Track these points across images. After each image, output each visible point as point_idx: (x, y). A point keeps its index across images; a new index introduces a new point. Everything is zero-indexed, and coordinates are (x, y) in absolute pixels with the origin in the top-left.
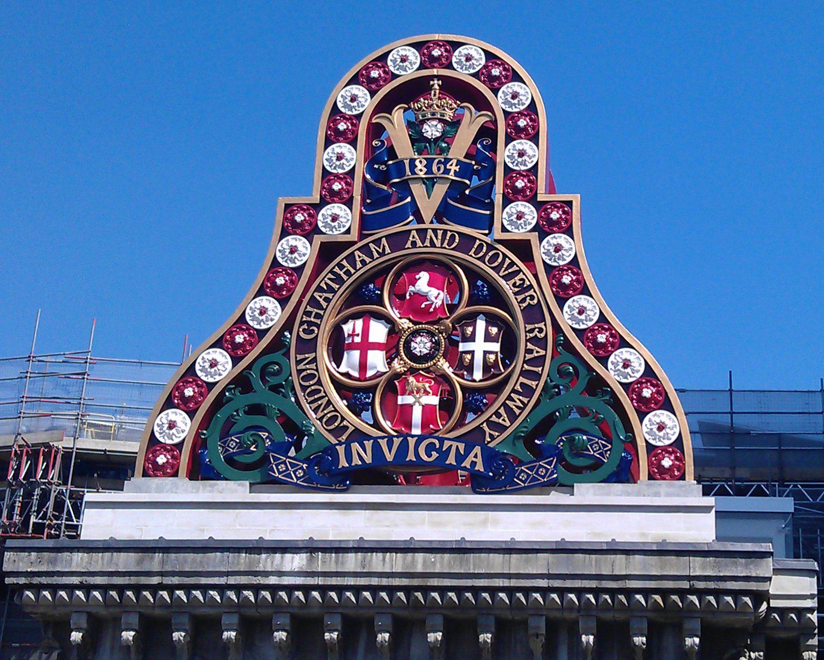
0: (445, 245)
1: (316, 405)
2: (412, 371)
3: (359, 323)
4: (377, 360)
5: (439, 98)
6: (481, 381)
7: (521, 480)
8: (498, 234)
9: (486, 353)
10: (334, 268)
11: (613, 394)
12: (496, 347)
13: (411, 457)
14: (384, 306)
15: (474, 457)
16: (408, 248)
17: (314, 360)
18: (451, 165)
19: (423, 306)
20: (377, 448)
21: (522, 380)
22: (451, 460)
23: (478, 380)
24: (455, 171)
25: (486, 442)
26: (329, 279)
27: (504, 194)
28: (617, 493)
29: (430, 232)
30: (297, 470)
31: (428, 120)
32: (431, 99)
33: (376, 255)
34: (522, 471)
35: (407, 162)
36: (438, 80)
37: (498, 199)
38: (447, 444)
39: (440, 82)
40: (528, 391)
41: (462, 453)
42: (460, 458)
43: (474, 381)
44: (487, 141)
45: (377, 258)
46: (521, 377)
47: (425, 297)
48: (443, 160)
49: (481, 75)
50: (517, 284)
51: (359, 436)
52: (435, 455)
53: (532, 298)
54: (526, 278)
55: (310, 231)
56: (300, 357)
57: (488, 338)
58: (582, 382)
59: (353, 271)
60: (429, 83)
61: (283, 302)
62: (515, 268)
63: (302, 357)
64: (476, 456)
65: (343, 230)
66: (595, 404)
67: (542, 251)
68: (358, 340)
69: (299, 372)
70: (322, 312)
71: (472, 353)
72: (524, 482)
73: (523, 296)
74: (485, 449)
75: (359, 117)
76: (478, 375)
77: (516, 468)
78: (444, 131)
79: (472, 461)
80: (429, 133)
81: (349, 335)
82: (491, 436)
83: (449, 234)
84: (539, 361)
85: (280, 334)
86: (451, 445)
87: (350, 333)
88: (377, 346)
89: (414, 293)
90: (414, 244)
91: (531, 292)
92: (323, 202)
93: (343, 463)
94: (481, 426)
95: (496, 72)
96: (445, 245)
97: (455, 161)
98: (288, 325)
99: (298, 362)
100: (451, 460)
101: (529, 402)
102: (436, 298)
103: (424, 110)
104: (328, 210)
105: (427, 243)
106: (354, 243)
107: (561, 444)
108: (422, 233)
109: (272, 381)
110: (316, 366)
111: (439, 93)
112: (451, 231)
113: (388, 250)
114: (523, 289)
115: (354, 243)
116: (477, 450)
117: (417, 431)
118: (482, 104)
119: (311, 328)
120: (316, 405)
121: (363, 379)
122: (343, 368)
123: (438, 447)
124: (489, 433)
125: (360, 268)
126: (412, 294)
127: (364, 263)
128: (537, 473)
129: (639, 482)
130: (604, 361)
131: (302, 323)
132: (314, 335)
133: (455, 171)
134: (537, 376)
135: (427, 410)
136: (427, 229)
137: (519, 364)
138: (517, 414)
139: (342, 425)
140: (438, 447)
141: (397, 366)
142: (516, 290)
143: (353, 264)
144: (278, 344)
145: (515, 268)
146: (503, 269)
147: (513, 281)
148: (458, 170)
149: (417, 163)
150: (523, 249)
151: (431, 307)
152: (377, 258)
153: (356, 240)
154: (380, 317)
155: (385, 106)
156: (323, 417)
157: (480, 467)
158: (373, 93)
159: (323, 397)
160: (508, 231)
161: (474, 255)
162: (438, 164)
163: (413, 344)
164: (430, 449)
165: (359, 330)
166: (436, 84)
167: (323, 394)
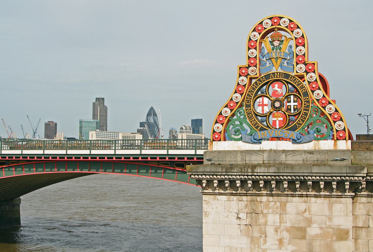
3: (261, 98)
8: (295, 73)
9: (294, 106)
11: (326, 116)
31: (275, 40)
37: (295, 64)
57: (294, 102)
62: (300, 82)
63: (247, 108)
65: (255, 74)
67: (307, 78)
68: (261, 103)
69: (247, 112)
71: (290, 106)
75: (256, 41)
76: (292, 111)
80: (275, 45)
85: (242, 102)
92: (249, 66)
98: (243, 100)
99: (246, 110)
104: (251, 69)
144: (241, 106)
147: (300, 86)
150: (302, 77)
158: (260, 34)
160: (298, 73)
165: (261, 101)
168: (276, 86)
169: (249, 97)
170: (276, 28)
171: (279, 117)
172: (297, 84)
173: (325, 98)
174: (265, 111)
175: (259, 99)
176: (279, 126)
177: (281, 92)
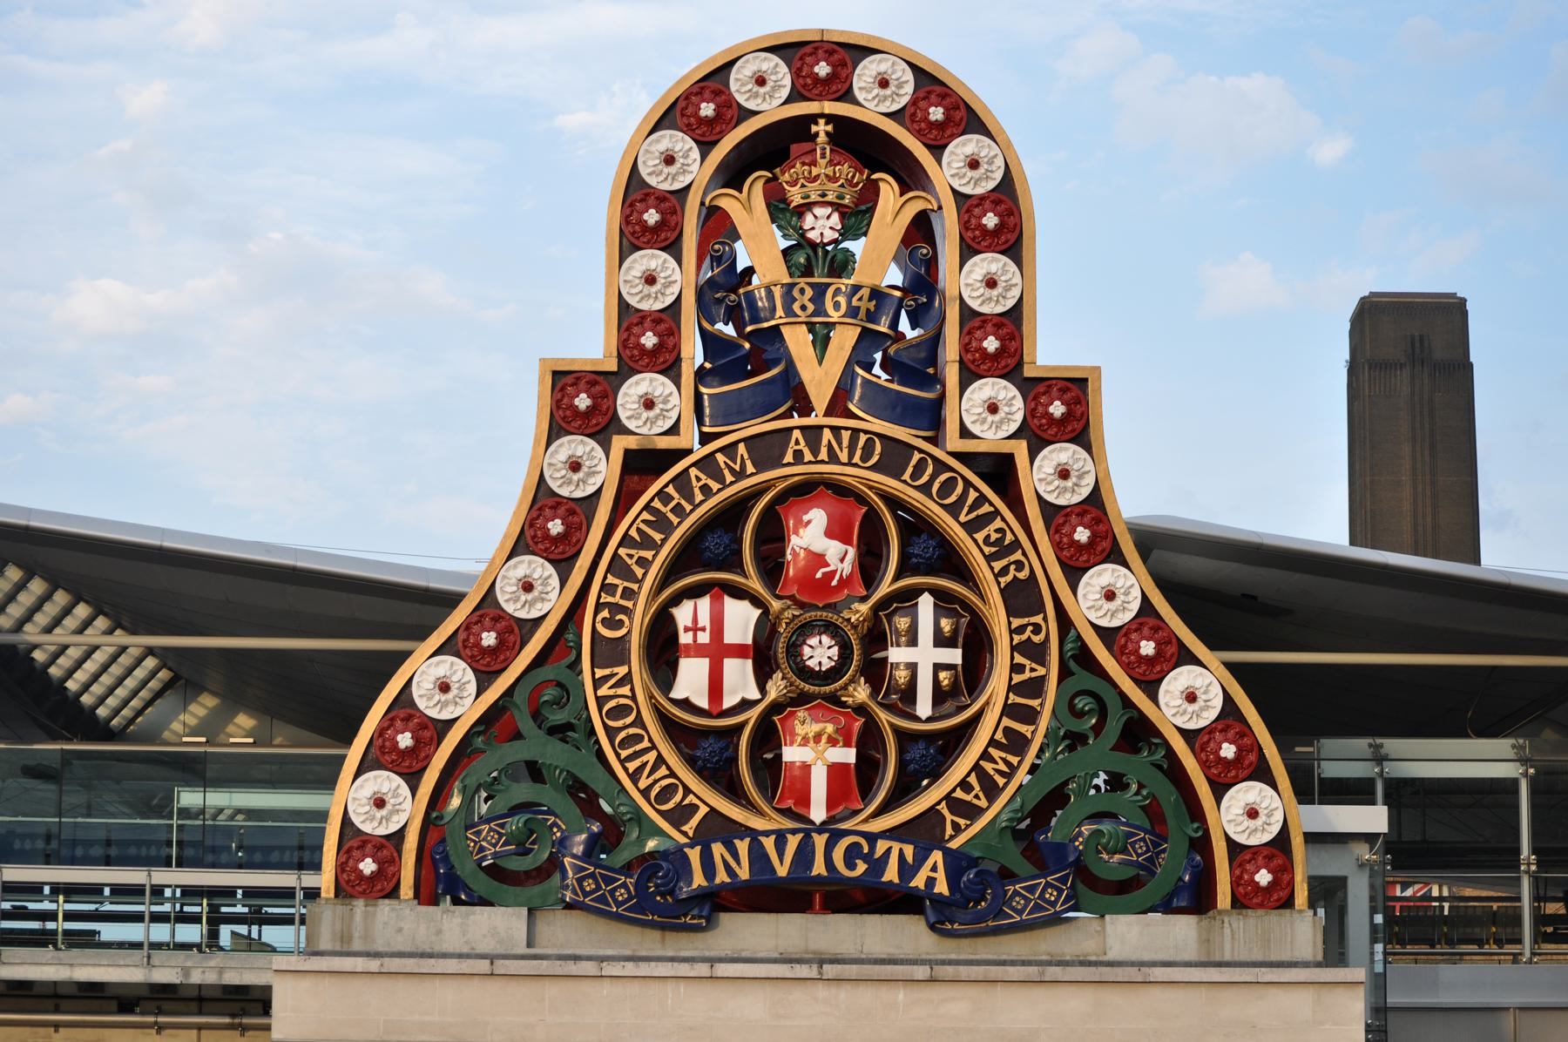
0: (856, 459)
2: (801, 699)
4: (740, 680)
5: (831, 163)
6: (929, 720)
7: (1013, 909)
8: (954, 442)
9: (938, 667)
10: (652, 500)
12: (955, 656)
13: (819, 868)
15: (931, 870)
16: (789, 464)
17: (627, 679)
18: (860, 299)
19: (819, 575)
20: (757, 854)
21: (1006, 722)
22: (891, 874)
23: (924, 717)
24: (868, 310)
25: (947, 837)
26: (643, 521)
27: (961, 362)
28: (1180, 932)
29: (827, 434)
30: (615, 889)
33: (729, 478)
34: (1016, 893)
36: (827, 124)
37: (952, 375)
38: (881, 846)
39: (830, 128)
40: (1016, 744)
41: (910, 859)
42: (907, 871)
43: (917, 719)
44: (925, 251)
45: (732, 483)
46: (1004, 719)
47: (819, 559)
48: (844, 289)
50: (992, 539)
51: (718, 829)
52: (861, 867)
53: (1019, 565)
54: (1006, 528)
55: (602, 425)
56: (599, 673)
57: (941, 641)
59: (688, 508)
61: (563, 566)
62: (986, 508)
63: (607, 672)
64: (934, 869)
65: (669, 424)
66: (1137, 767)
68: (704, 638)
69: (601, 702)
70: (635, 587)
72: (1020, 913)
73: (1004, 562)
74: (947, 853)
76: (924, 707)
79: (928, 877)
81: (687, 629)
82: (956, 826)
83: (863, 438)
84: (1035, 687)
86: (889, 850)
87: (690, 624)
88: (739, 651)
90: (798, 455)
91: (1018, 556)
93: (699, 880)
95: (937, 113)
96: (856, 459)
97: (865, 292)
99: (597, 684)
100: (891, 874)
101: (1020, 763)
102: (842, 560)
105: (823, 455)
107: (1081, 839)
108: (812, 433)
109: (557, 717)
110: (632, 690)
111: (831, 150)
112: (866, 432)
113: (750, 469)
114: (1002, 549)
116: (937, 856)
117: (818, 813)
118: (911, 177)
119: (618, 617)
121: (715, 713)
122: (677, 693)
123: (866, 850)
124: (952, 821)
125: (702, 502)
127: (706, 490)
128: (1041, 896)
130: (1151, 688)
131: (599, 607)
132: (623, 631)
133: (868, 310)
134: (1030, 716)
135: (836, 771)
136: (821, 427)
137: (997, 684)
138: (1001, 785)
139: (686, 802)
140: (866, 850)
141: (776, 687)
142: (993, 549)
143: (689, 497)
145: (986, 508)
146: (966, 509)
148: (872, 309)
149: (796, 293)
150: (999, 471)
151: (833, 578)
152: (732, 483)
154: (739, 593)
155: (733, 175)
157: (942, 887)
159: (646, 751)
161: (909, 481)
162: (834, 296)
163: (807, 651)
164: (852, 854)
165: (704, 620)
166: (821, 128)
167: (646, 744)
168: (817, 518)
170: (822, 115)
171: (832, 742)
172: (963, 518)
173: (1152, 621)
174: (734, 692)
176: (830, 805)
177: (846, 568)
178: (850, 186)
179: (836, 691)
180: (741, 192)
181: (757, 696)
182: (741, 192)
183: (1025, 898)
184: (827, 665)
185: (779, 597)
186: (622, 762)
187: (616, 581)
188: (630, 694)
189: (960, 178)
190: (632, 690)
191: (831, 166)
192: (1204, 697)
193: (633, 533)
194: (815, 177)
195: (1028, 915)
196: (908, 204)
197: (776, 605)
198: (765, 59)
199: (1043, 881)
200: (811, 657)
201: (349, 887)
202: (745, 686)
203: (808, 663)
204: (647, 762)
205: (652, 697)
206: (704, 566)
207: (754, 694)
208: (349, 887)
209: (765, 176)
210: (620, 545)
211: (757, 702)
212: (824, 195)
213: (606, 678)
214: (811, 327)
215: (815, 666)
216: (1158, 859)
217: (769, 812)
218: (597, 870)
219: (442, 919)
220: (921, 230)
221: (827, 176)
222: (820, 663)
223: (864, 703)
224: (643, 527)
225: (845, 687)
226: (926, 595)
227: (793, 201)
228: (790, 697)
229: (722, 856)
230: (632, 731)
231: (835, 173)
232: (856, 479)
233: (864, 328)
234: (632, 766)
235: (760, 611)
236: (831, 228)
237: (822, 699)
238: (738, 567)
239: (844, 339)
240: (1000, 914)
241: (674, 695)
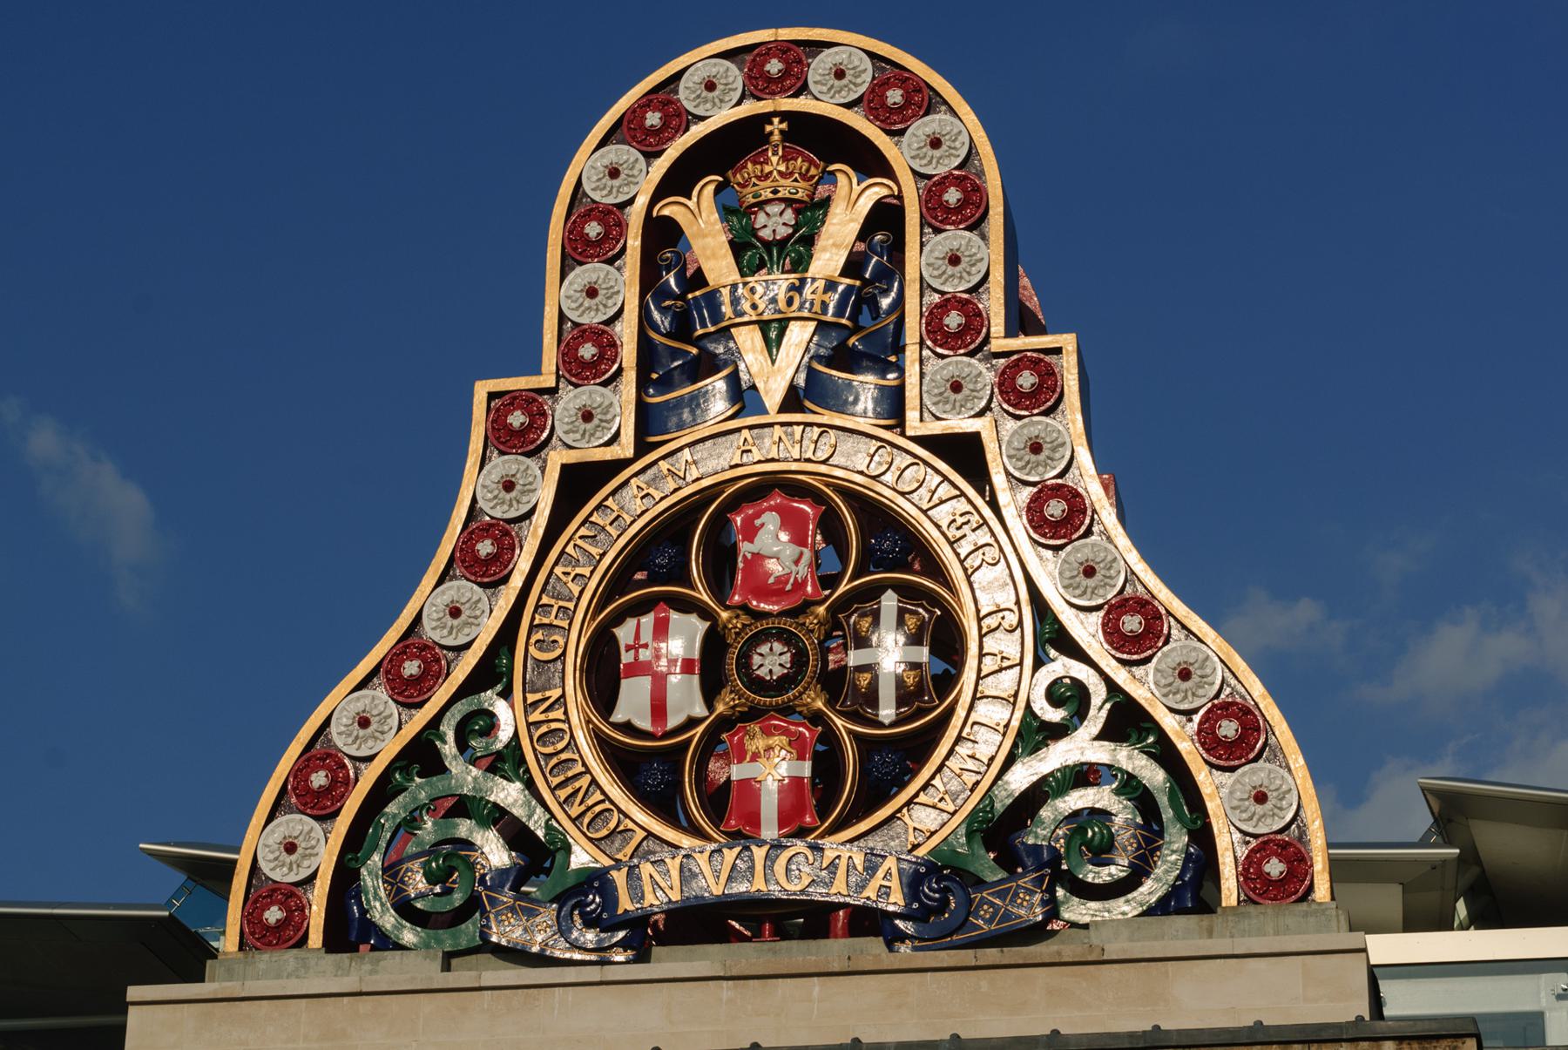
1: (569, 790)
2: (753, 714)
4: (685, 699)
14: (693, 587)
23: (887, 722)
26: (581, 537)
32: (767, 161)
34: (983, 901)
35: (725, 292)
36: (781, 122)
39: (784, 126)
43: (881, 725)
48: (797, 283)
49: (871, 103)
58: (1097, 718)
60: (764, 129)
63: (538, 696)
76: (887, 713)
77: (972, 896)
78: (796, 223)
81: (628, 648)
89: (753, 554)
93: (626, 904)
94: (899, 815)
102: (797, 562)
103: (755, 185)
106: (626, 463)
110: (566, 713)
111: (784, 147)
115: (626, 463)
118: (871, 163)
120: (569, 790)
122: (619, 716)
126: (749, 556)
129: (1219, 910)
139: (621, 828)
153: (629, 452)
154: (687, 606)
155: (678, 182)
156: (583, 814)
163: (756, 660)
166: (776, 127)
167: (579, 768)
169: (557, 604)
175: (631, 623)
178: (804, 180)
179: (789, 700)
180: (690, 199)
181: (707, 714)
182: (690, 199)
183: (992, 904)
184: (778, 672)
185: (727, 608)
186: (553, 790)
187: (552, 602)
188: (563, 717)
189: (921, 159)
190: (566, 713)
191: (783, 162)
192: (1199, 672)
193: (570, 549)
194: (767, 175)
195: (997, 924)
196: (868, 193)
197: (725, 615)
198: (715, 65)
199: (1015, 884)
200: (761, 665)
201: (258, 937)
202: (692, 705)
203: (758, 672)
204: (580, 788)
205: (589, 721)
206: (1230, 1031)
207: (699, 710)
208: (258, 937)
209: (717, 181)
210: (556, 563)
211: (707, 718)
212: (775, 192)
213: (535, 704)
214: (764, 326)
215: (766, 675)
216: (1152, 858)
217: (715, 836)
218: (519, 902)
219: (350, 965)
220: (886, 218)
221: (780, 172)
222: (771, 671)
223: (820, 710)
224: (579, 542)
225: (801, 694)
226: (890, 592)
227: (744, 202)
228: (739, 711)
229: (651, 876)
230: (564, 756)
231: (787, 168)
232: (812, 477)
233: (819, 321)
234: (563, 794)
235: (708, 624)
236: (784, 224)
237: (775, 711)
238: (688, 583)
239: (799, 335)
240: (963, 925)
241: (612, 719)
